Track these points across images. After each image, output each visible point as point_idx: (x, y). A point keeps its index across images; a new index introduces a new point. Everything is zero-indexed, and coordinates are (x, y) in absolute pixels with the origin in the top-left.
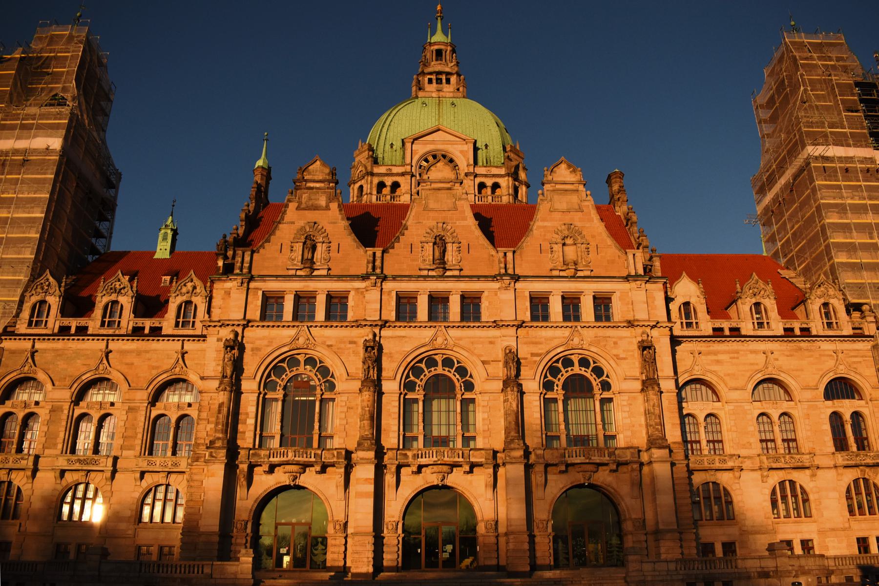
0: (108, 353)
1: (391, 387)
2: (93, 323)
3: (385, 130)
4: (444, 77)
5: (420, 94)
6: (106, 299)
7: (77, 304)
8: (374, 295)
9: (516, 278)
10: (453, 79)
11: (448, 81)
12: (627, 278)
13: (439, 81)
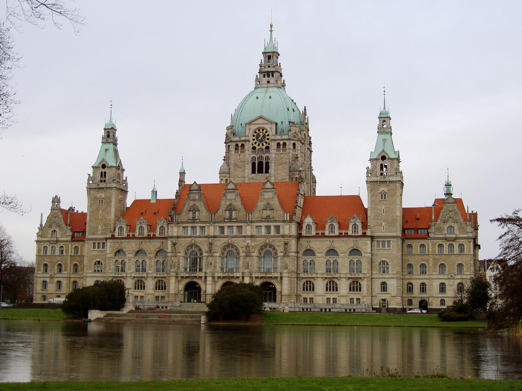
3: (239, 116)
5: (259, 86)
6: (139, 226)
7: (132, 228)
8: (212, 228)
9: (252, 222)
10: (276, 75)
11: (273, 76)
12: (284, 221)
13: (269, 76)
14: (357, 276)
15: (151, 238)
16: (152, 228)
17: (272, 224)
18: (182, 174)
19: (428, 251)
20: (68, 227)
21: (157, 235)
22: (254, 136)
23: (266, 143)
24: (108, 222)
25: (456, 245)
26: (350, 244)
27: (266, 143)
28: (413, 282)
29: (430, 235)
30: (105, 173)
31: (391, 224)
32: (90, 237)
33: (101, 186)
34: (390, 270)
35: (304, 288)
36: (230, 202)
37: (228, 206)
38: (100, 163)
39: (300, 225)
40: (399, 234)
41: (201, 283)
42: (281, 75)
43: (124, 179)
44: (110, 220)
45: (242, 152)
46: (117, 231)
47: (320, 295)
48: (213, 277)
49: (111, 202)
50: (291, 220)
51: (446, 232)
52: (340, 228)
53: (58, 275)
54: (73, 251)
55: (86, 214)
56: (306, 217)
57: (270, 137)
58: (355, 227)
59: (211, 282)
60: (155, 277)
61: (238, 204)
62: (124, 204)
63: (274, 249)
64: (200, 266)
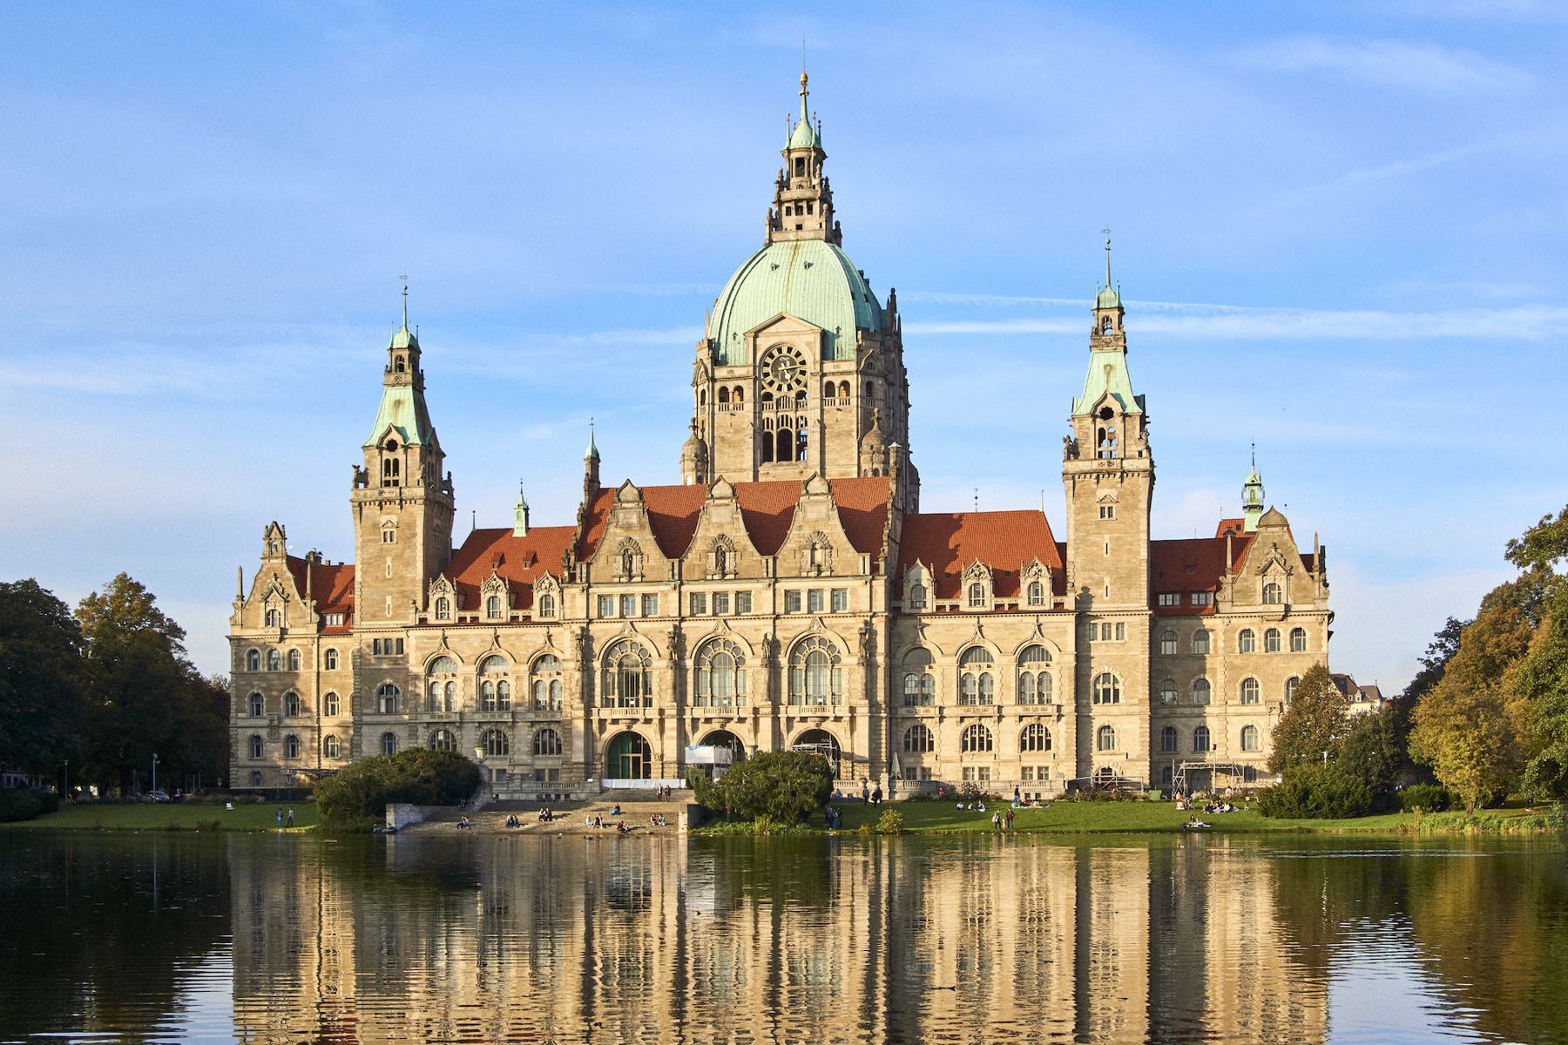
0: (497, 638)
1: (689, 663)
2: (482, 615)
4: (804, 204)
5: (776, 236)
7: (469, 598)
10: (816, 206)
13: (799, 210)
14: (1040, 712)
15: (519, 625)
16: (520, 596)
17: (827, 585)
18: (595, 460)
19: (1215, 647)
20: (308, 601)
21: (535, 617)
22: (767, 365)
23: (798, 382)
24: (408, 587)
25: (1284, 630)
26: (1023, 629)
27: (798, 382)
28: (1178, 724)
29: (1221, 606)
30: (396, 461)
31: (1124, 580)
32: (365, 624)
33: (386, 495)
35: (907, 744)
36: (720, 532)
37: (715, 541)
38: (382, 439)
39: (895, 591)
40: (1143, 604)
41: (649, 733)
42: (831, 211)
43: (445, 477)
44: (413, 580)
45: (741, 407)
46: (432, 608)
47: (946, 762)
48: (681, 721)
49: (414, 535)
51: (1259, 599)
52: (998, 592)
53: (288, 722)
54: (323, 660)
55: (352, 568)
56: (912, 564)
57: (811, 367)
58: (1035, 588)
59: (675, 734)
60: (533, 723)
61: (740, 535)
62: (448, 541)
63: (832, 647)
64: (645, 693)
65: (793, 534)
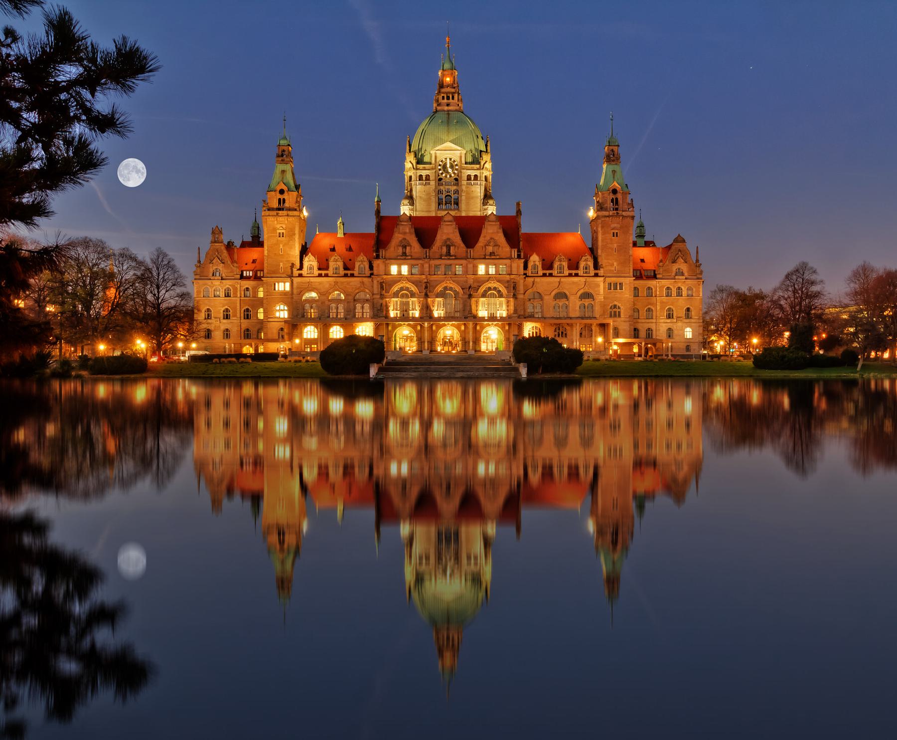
30: (284, 200)
34: (622, 315)
49: (294, 234)
50: (519, 257)
61: (457, 238)
65: (481, 239)
